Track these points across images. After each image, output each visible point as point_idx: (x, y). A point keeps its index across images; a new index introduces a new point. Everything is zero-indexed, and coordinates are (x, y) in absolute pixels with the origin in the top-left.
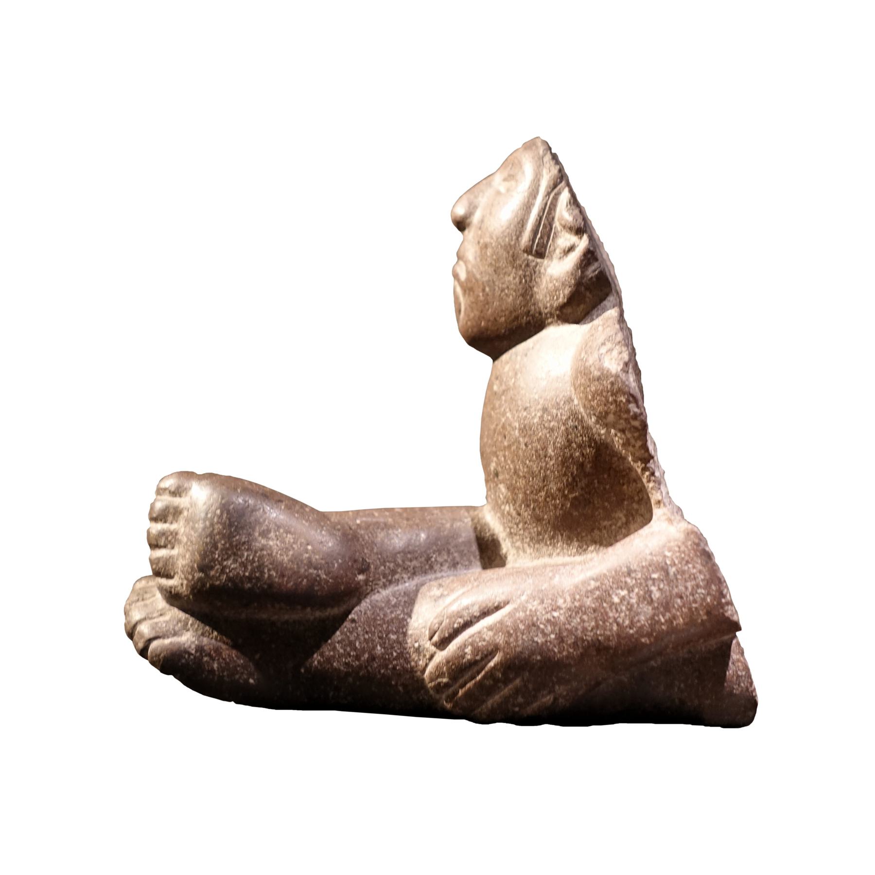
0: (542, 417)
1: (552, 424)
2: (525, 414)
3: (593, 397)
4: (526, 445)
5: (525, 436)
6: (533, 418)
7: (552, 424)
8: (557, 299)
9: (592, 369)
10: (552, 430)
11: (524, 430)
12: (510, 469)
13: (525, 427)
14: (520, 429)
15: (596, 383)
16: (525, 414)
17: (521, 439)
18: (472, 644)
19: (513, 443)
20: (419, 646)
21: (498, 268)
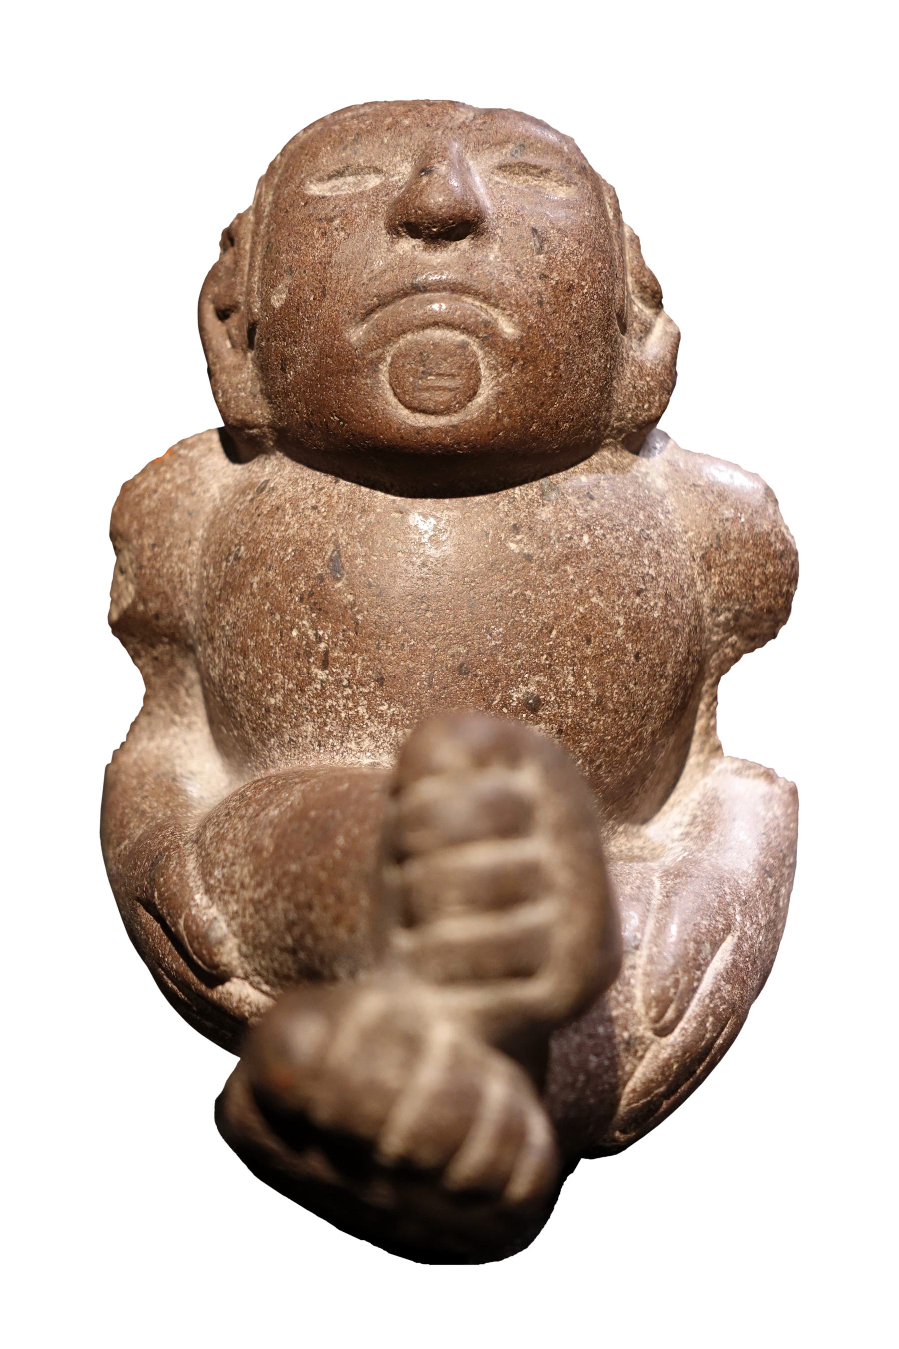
0: (664, 609)
1: (676, 621)
2: (638, 600)
3: (764, 583)
4: (637, 657)
5: (638, 640)
6: (653, 609)
7: (676, 621)
8: (649, 409)
9: (772, 539)
10: (676, 631)
11: (638, 627)
12: (588, 697)
13: (639, 623)
14: (627, 628)
15: (777, 561)
16: (638, 600)
17: (629, 645)
18: (714, 1014)
19: (610, 652)
20: (630, 1036)
21: (587, 333)
